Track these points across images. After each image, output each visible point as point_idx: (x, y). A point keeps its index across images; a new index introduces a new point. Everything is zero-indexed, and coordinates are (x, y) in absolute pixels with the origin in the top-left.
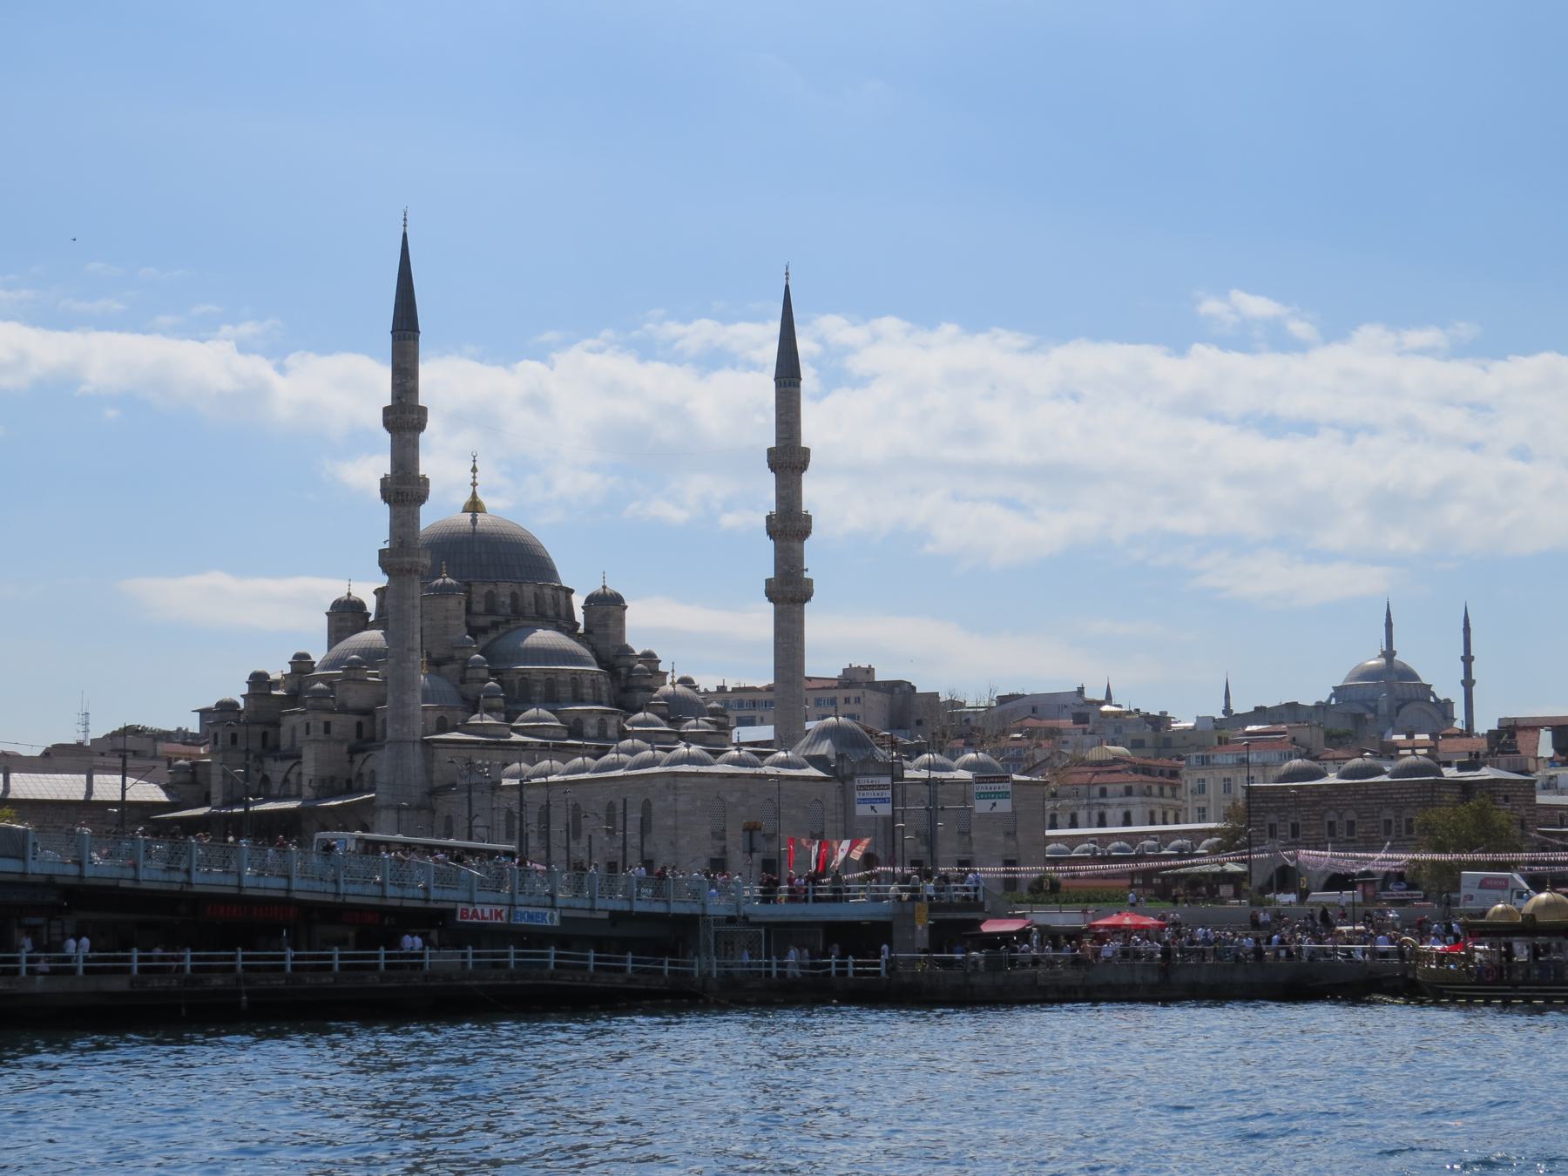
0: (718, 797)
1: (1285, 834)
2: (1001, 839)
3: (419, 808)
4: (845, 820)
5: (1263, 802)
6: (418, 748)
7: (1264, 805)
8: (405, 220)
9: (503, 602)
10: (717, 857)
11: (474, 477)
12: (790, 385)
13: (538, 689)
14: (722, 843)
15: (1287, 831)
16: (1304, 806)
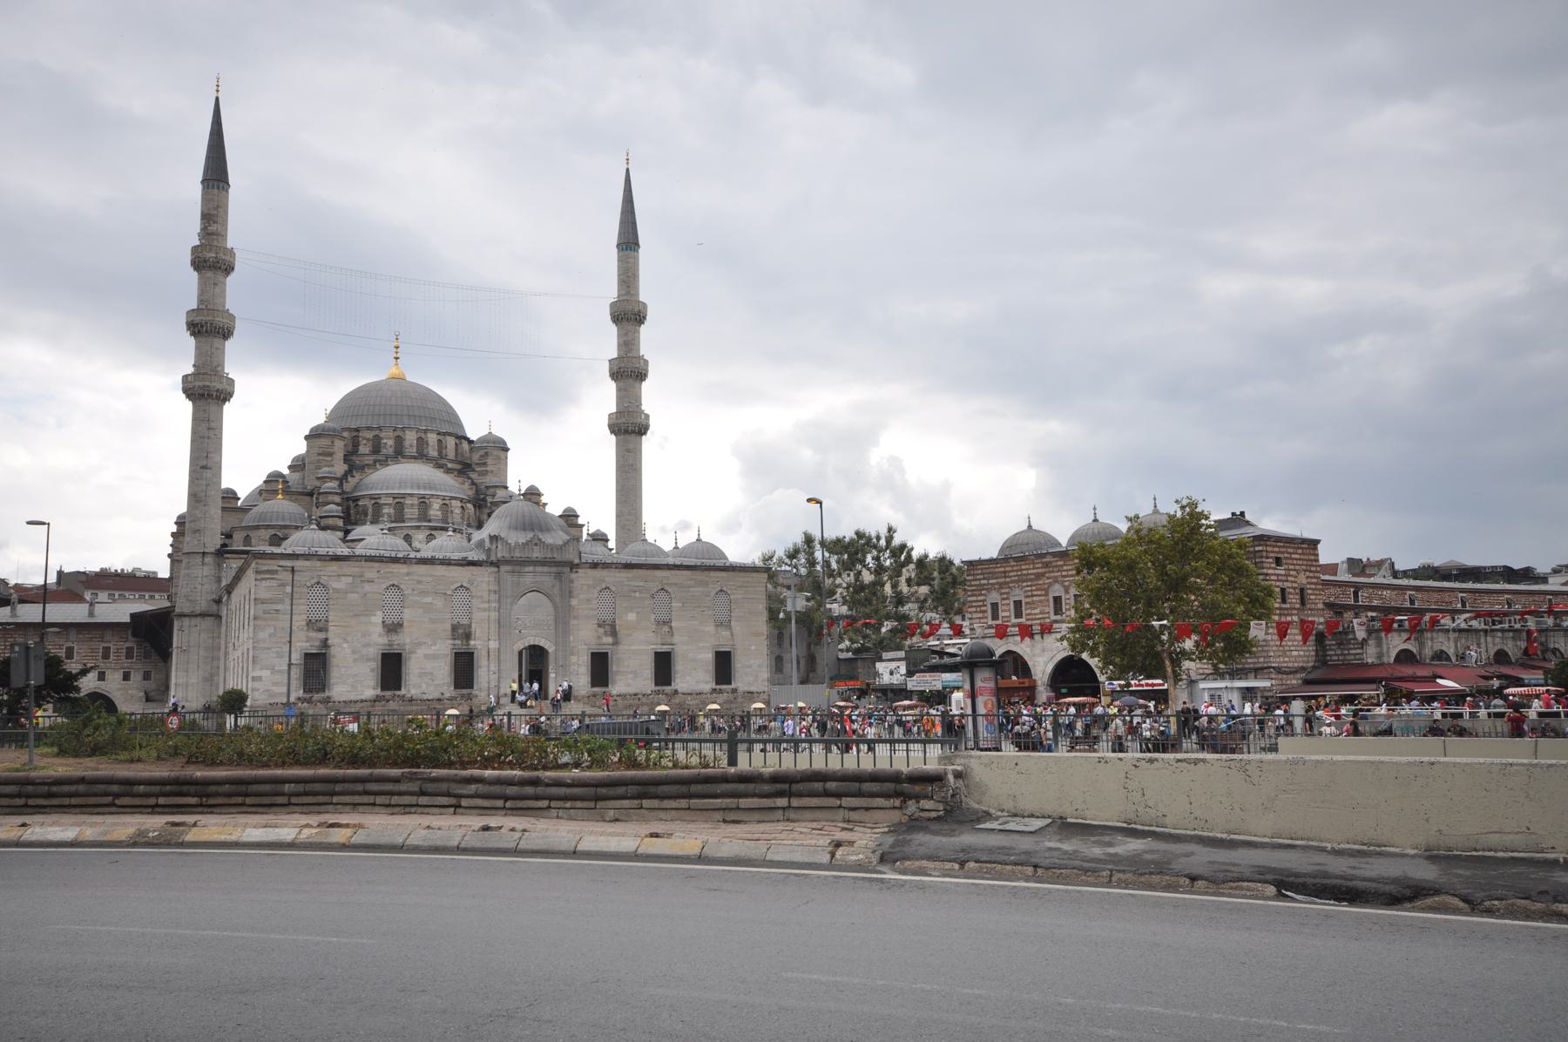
0: (318, 583)
1: (1007, 614)
2: (711, 628)
3: (203, 615)
4: (499, 608)
5: (984, 579)
6: (208, 559)
7: (985, 582)
8: (218, 86)
9: (386, 444)
10: (314, 651)
11: (397, 353)
12: (627, 249)
13: (386, 511)
14: (322, 636)
15: (1009, 610)
16: (1027, 581)
